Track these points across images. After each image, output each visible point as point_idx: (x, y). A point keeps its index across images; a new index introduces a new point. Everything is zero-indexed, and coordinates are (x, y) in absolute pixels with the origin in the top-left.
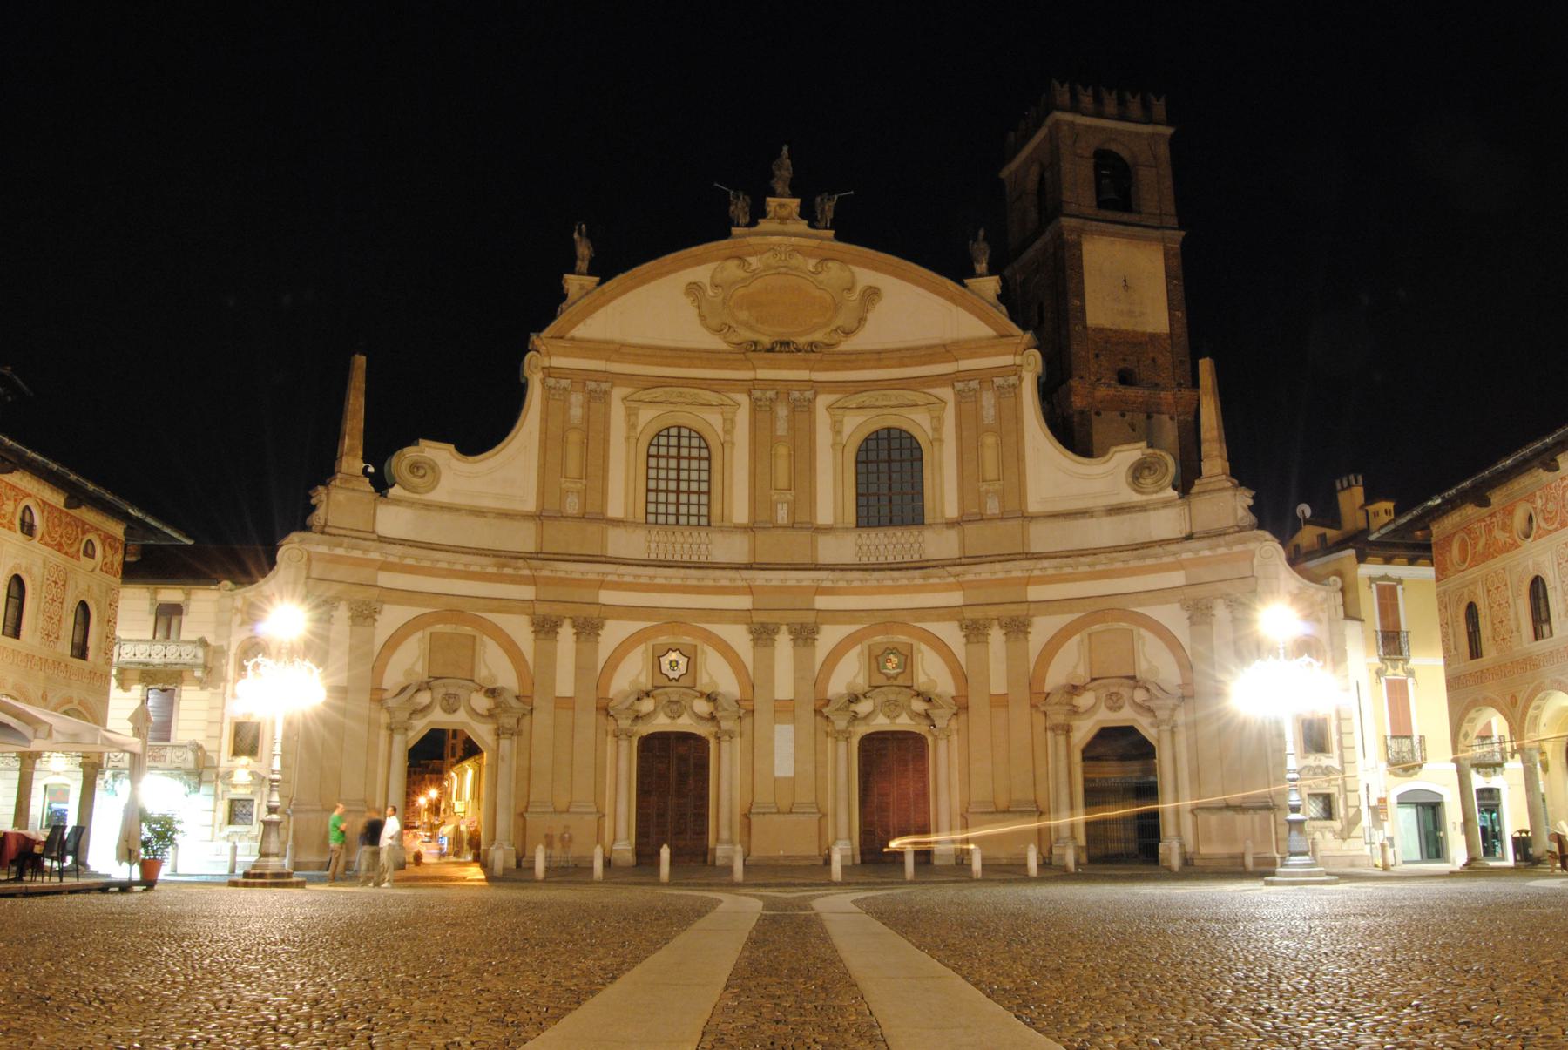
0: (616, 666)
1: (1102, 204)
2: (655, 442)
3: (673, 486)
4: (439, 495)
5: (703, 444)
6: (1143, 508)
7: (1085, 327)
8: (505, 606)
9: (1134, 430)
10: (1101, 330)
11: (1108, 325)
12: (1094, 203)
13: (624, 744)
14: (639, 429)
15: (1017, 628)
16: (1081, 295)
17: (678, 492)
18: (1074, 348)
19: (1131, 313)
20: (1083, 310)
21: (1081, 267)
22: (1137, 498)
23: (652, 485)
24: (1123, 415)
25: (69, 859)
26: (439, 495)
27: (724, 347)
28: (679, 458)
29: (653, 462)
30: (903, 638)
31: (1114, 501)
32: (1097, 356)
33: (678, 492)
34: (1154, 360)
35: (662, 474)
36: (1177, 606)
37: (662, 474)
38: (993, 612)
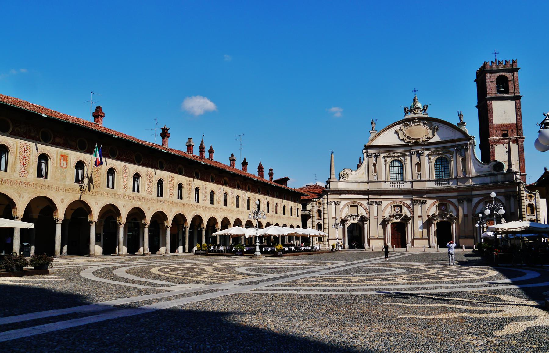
0: (386, 210)
1: (499, 92)
2: (391, 164)
3: (395, 173)
4: (349, 179)
5: (401, 163)
6: (497, 175)
7: (493, 125)
8: (363, 199)
9: (506, 148)
10: (497, 125)
11: (499, 123)
12: (496, 92)
13: (388, 225)
14: (387, 161)
15: (470, 200)
16: (492, 117)
17: (396, 174)
18: (490, 130)
19: (506, 119)
20: (492, 120)
21: (492, 110)
22: (495, 172)
23: (391, 173)
24: (503, 145)
25: (263, 250)
26: (349, 179)
27: (404, 144)
28: (396, 167)
29: (391, 168)
30: (445, 202)
31: (490, 173)
32: (496, 131)
33: (396, 174)
34: (512, 130)
35: (393, 170)
36: (503, 196)
37: (393, 170)
38: (465, 197)
